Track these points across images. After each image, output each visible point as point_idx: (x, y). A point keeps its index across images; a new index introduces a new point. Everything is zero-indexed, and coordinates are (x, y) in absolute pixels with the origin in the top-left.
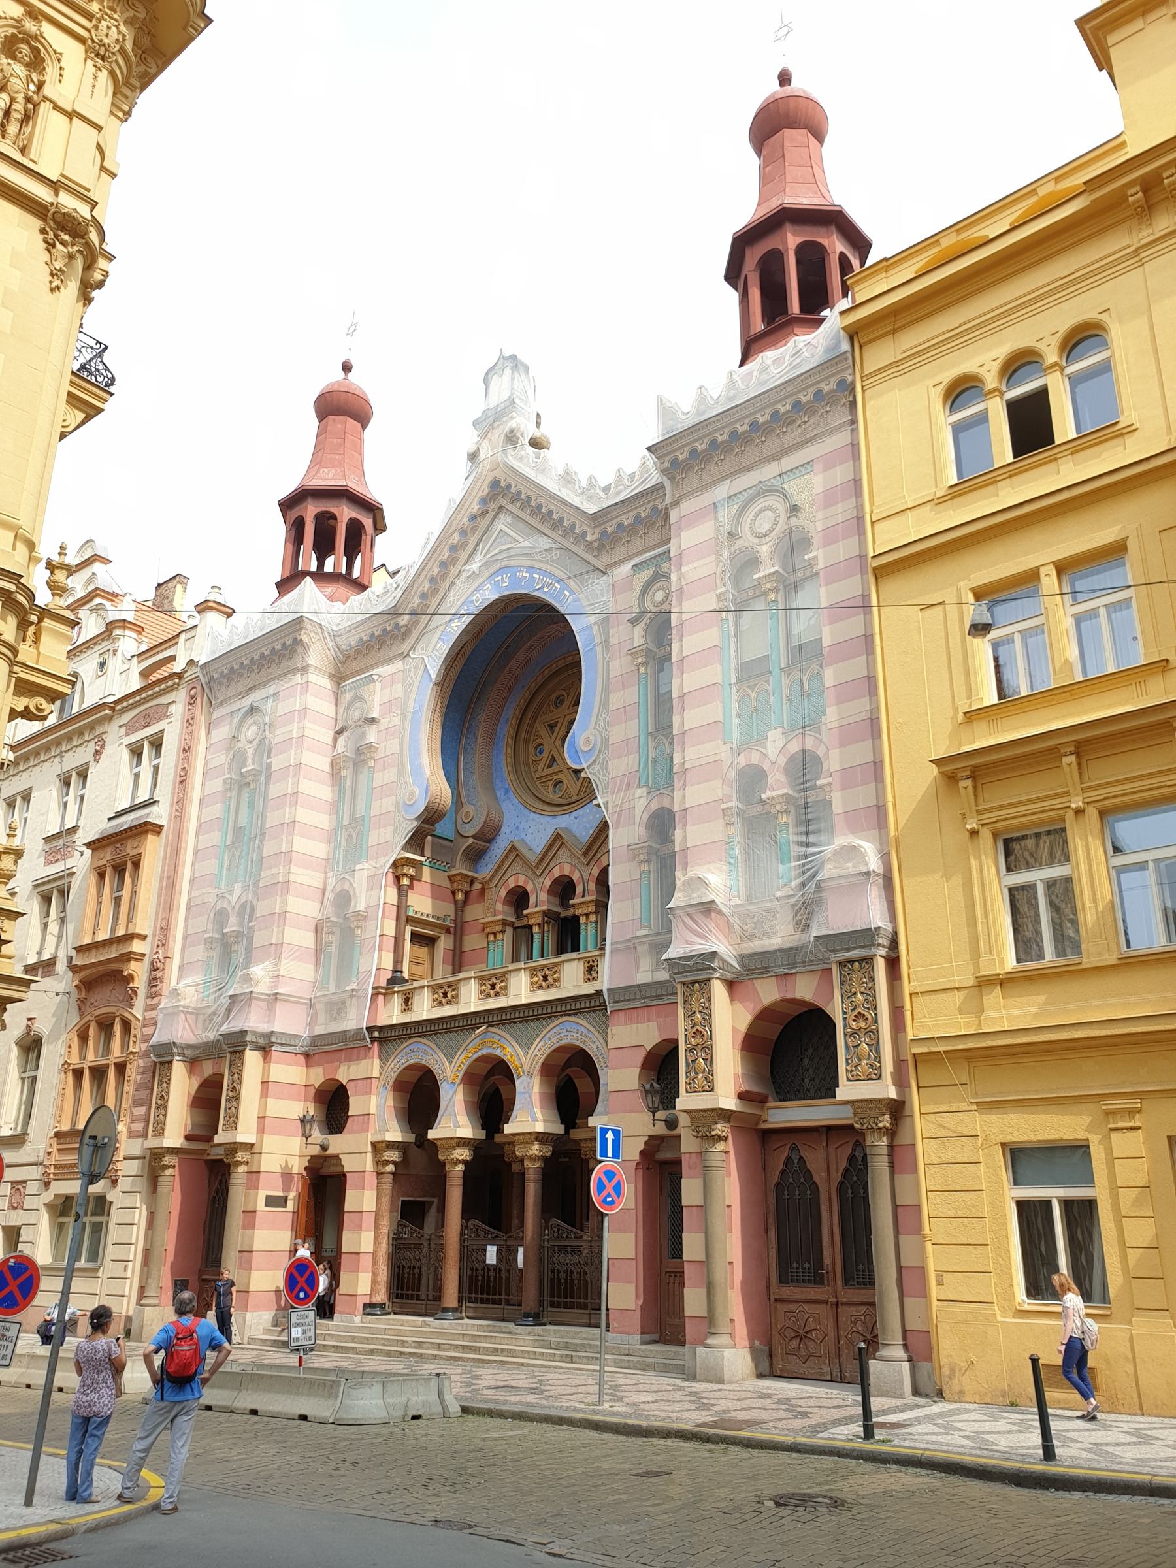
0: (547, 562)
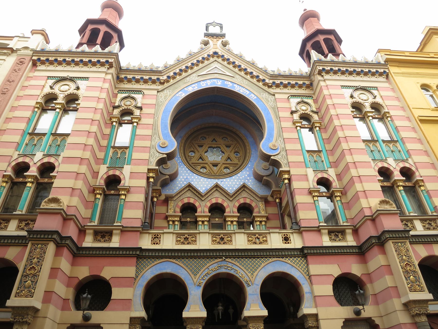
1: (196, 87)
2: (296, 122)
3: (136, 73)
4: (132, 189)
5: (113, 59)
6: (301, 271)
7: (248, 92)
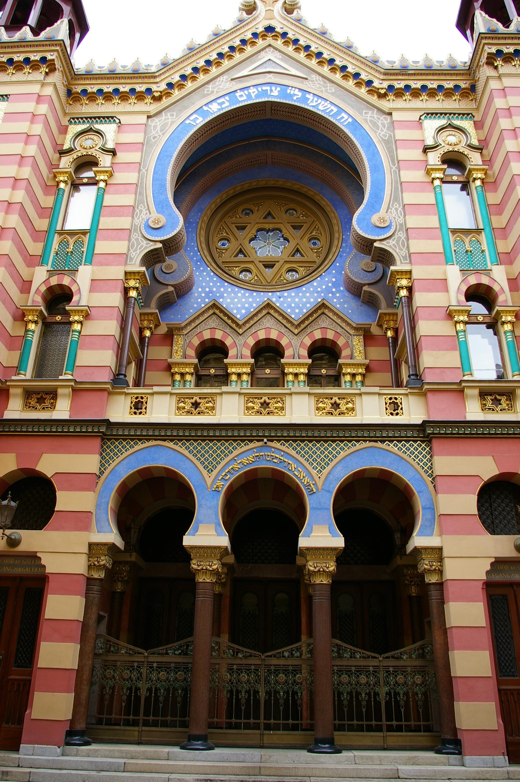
0: (322, 91)
1: (227, 104)
2: (432, 169)
3: (105, 81)
4: (93, 312)
5: (56, 54)
6: (418, 467)
7: (335, 110)
